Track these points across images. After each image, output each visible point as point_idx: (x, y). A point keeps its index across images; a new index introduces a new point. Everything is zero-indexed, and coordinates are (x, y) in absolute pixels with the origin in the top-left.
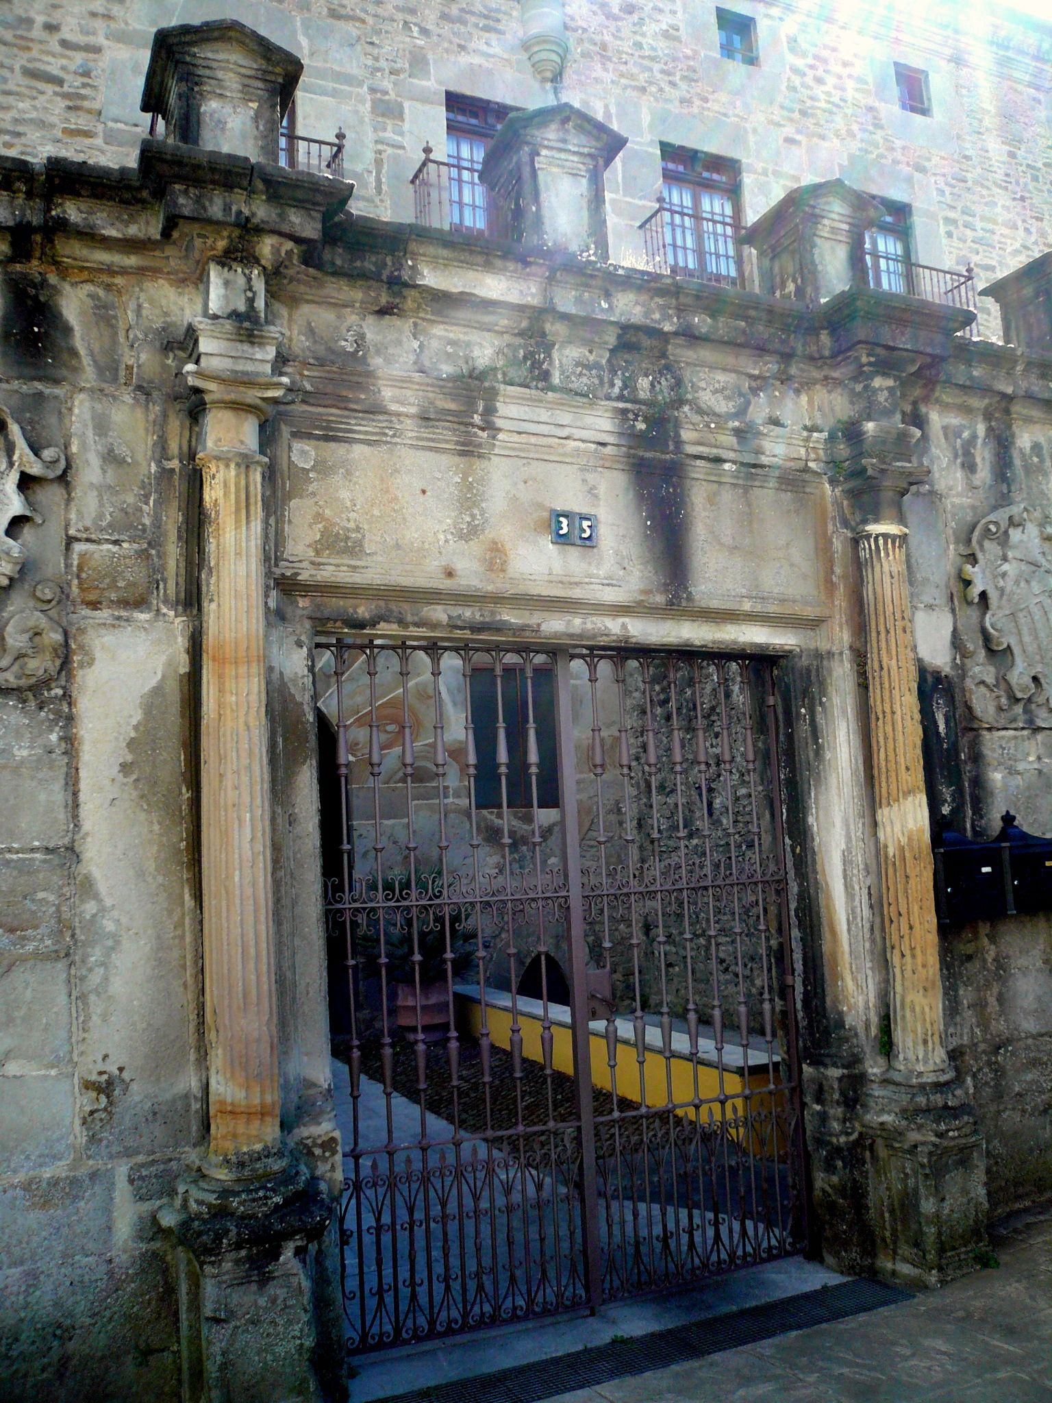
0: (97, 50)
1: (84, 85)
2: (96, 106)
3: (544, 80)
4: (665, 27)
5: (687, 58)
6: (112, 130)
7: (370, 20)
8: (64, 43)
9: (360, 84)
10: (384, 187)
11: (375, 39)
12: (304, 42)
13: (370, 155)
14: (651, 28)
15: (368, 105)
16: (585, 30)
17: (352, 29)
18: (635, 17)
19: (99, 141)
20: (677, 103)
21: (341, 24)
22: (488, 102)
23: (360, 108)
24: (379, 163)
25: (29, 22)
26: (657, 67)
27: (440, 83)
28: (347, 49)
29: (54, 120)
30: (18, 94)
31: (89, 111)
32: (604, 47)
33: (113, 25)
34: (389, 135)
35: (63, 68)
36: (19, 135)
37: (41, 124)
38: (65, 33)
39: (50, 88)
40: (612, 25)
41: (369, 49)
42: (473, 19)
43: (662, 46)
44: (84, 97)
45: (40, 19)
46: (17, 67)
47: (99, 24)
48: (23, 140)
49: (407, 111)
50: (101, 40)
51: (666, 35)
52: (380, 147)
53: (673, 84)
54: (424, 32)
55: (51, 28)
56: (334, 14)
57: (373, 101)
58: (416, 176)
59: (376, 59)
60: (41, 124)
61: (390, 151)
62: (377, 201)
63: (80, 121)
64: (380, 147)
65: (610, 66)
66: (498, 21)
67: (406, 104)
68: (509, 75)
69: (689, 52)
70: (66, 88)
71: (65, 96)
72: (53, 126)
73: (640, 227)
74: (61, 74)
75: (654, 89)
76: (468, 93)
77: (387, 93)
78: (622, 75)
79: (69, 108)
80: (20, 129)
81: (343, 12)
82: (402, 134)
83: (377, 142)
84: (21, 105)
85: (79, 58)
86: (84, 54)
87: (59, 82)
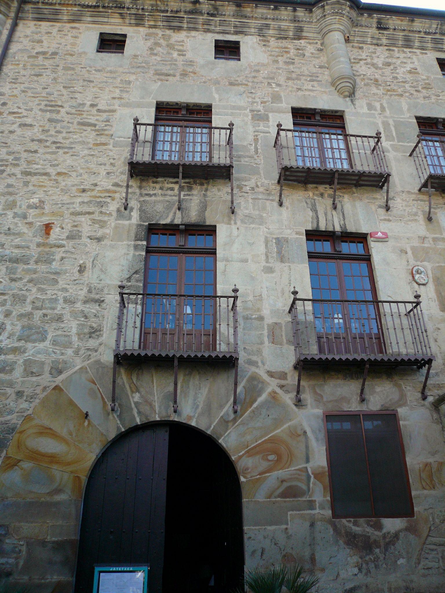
0: (114, 111)
1: (106, 126)
2: (111, 133)
3: (345, 97)
4: (409, 69)
5: (424, 80)
6: (117, 141)
7: (250, 84)
8: (99, 111)
9: (245, 109)
10: (259, 151)
11: (253, 91)
12: (216, 96)
13: (251, 138)
14: (401, 71)
15: (250, 117)
16: (364, 75)
17: (241, 89)
18: (392, 67)
19: (111, 147)
20: (422, 99)
21: (236, 87)
22: (315, 109)
23: (246, 119)
24: (256, 140)
25: (84, 104)
26: (407, 85)
27: (287, 104)
28: (239, 97)
29: (90, 140)
30: (74, 132)
31: (107, 135)
32: (376, 80)
33: (122, 101)
34: (261, 128)
35: (97, 120)
36: (72, 148)
37: (83, 143)
38: (100, 107)
39: (89, 129)
40: (380, 72)
41: (250, 95)
42: (304, 78)
43: (409, 77)
44: (105, 130)
45: (89, 103)
46: (75, 123)
47: (117, 102)
48: (74, 150)
49: (270, 117)
50: (116, 107)
51: (410, 72)
52: (256, 133)
53: (417, 91)
54: (278, 85)
55: (92, 106)
56: (231, 84)
57: (252, 115)
58: (276, 142)
59: (254, 98)
60: (83, 143)
61: (262, 134)
62: (255, 157)
63: (103, 139)
64: (256, 133)
65: (381, 88)
66: (318, 77)
67: (270, 115)
68: (325, 97)
69: (424, 77)
70: (97, 128)
71: (95, 131)
72: (88, 143)
73: (410, 155)
74: (96, 122)
75: (407, 94)
76: (303, 106)
77: (260, 111)
78: (388, 91)
79: (97, 135)
80: (73, 146)
81: (237, 83)
82: (268, 127)
83: (254, 132)
84: (75, 137)
85: (105, 115)
86: (108, 114)
87: (95, 125)
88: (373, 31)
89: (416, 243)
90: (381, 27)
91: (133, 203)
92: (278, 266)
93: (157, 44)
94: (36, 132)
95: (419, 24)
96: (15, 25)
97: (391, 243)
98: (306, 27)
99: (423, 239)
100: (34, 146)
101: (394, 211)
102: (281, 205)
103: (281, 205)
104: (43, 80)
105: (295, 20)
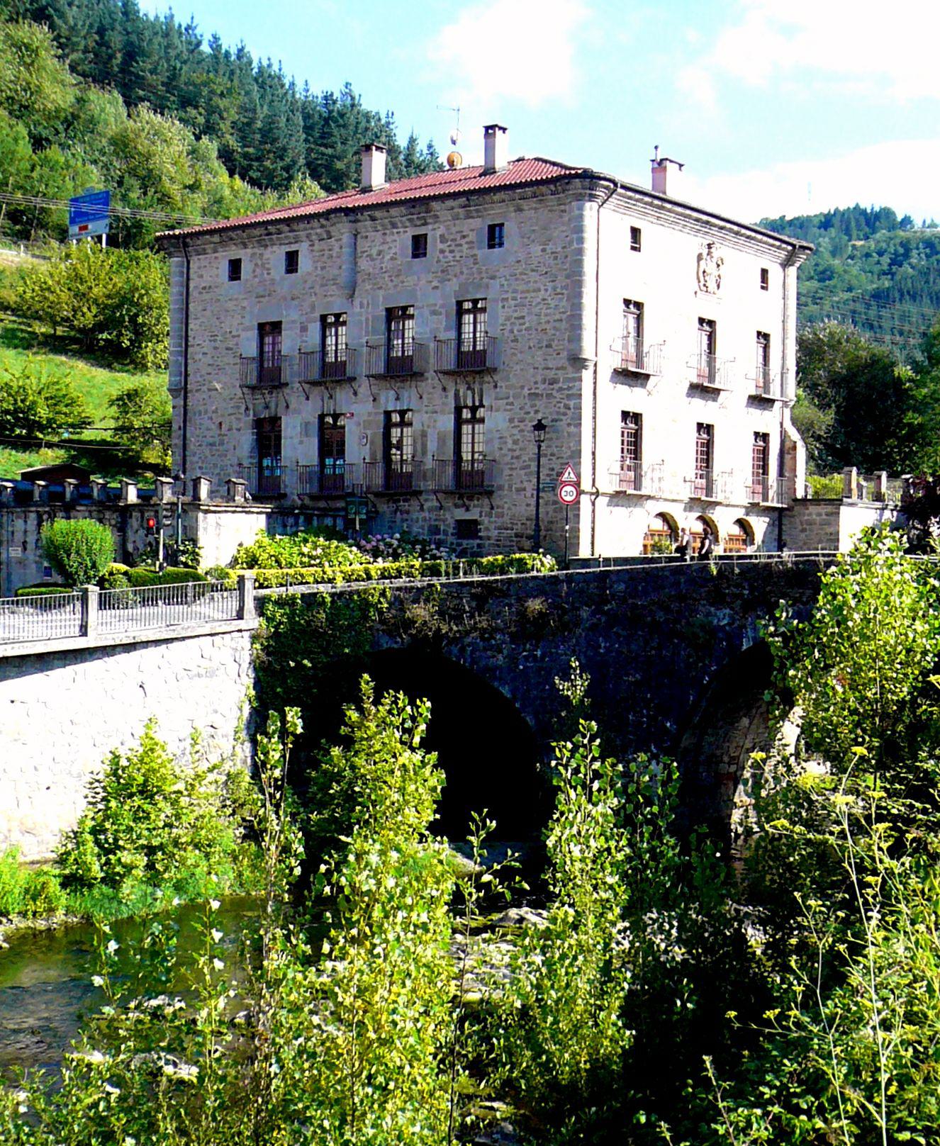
51: (392, 259)
56: (293, 299)
88: (369, 223)
89: (366, 418)
90: (373, 219)
91: (251, 406)
92: (305, 439)
93: (256, 265)
94: (208, 360)
95: (394, 211)
96: (188, 262)
97: (355, 418)
98: (331, 229)
99: (369, 414)
100: (209, 370)
101: (360, 395)
102: (308, 399)
103: (308, 399)
104: (208, 313)
105: (322, 226)
